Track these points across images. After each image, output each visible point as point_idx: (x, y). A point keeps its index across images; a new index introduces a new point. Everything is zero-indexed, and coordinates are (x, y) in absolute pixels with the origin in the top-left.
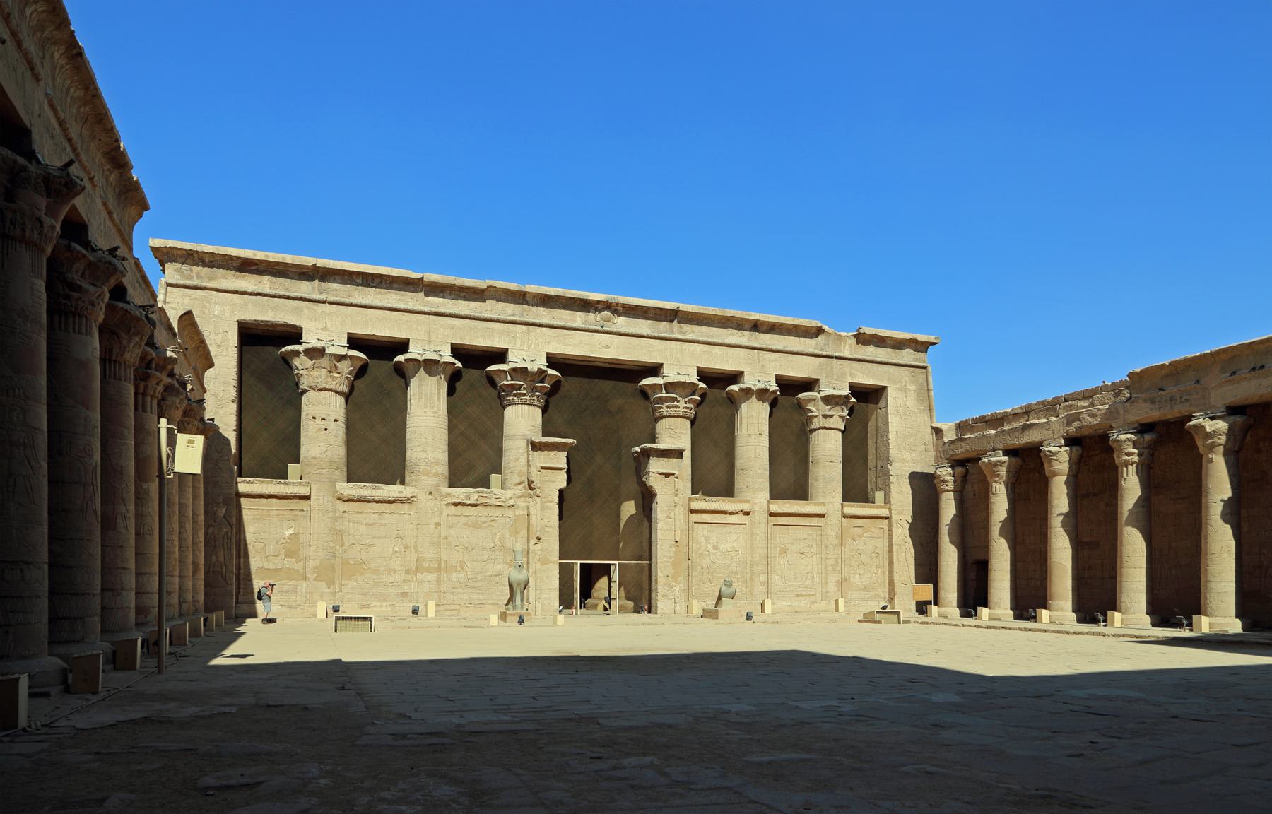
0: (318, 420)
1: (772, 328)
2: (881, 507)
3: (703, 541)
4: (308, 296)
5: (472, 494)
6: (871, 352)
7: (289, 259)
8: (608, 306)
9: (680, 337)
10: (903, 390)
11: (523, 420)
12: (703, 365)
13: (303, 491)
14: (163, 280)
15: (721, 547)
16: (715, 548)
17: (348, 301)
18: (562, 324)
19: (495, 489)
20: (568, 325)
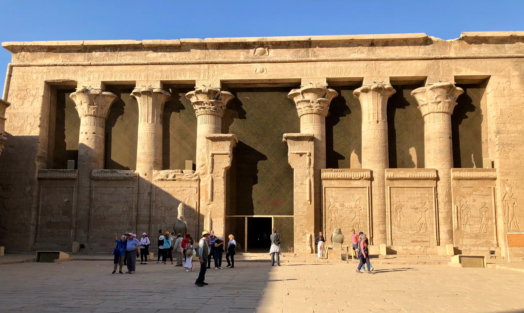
0: (84, 133)
1: (386, 43)
2: (488, 170)
3: (332, 200)
4: (81, 63)
5: (171, 173)
6: (474, 50)
7: (69, 43)
8: (261, 44)
9: (313, 59)
10: (508, 77)
11: (204, 126)
12: (330, 76)
13: (74, 175)
14: (9, 64)
15: (347, 204)
16: (342, 205)
17: (102, 63)
18: (230, 60)
19: (188, 171)
20: (234, 61)
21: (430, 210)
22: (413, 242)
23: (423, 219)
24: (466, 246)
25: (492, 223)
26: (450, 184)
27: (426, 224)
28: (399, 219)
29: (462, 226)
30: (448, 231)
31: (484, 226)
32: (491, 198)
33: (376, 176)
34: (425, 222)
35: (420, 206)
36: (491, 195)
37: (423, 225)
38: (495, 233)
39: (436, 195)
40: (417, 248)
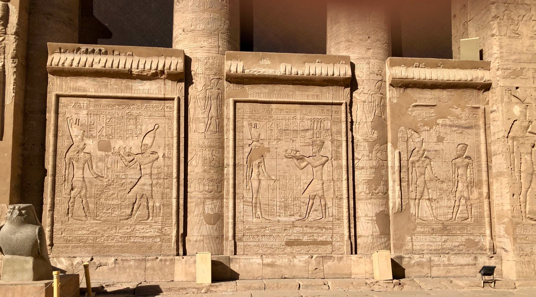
3: (75, 131)
15: (117, 144)
16: (105, 147)
21: (335, 163)
22: (289, 243)
23: (316, 185)
24: (421, 253)
25: (481, 194)
26: (383, 97)
27: (322, 197)
28: (255, 184)
29: (412, 203)
30: (377, 215)
31: (463, 201)
32: (478, 135)
33: (199, 71)
34: (320, 193)
35: (309, 151)
36: (476, 126)
37: (317, 201)
38: (487, 220)
39: (350, 125)
40: (300, 261)
